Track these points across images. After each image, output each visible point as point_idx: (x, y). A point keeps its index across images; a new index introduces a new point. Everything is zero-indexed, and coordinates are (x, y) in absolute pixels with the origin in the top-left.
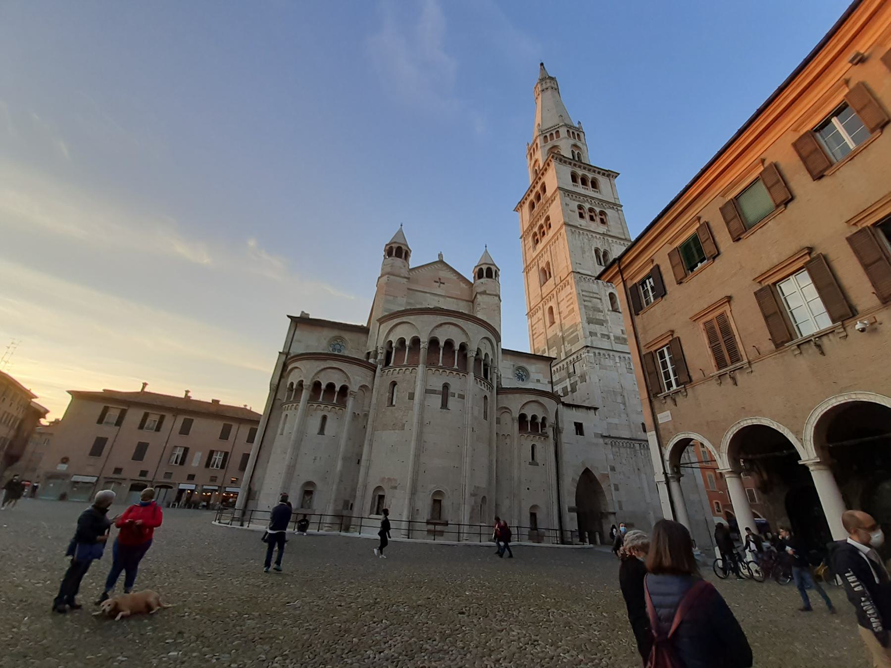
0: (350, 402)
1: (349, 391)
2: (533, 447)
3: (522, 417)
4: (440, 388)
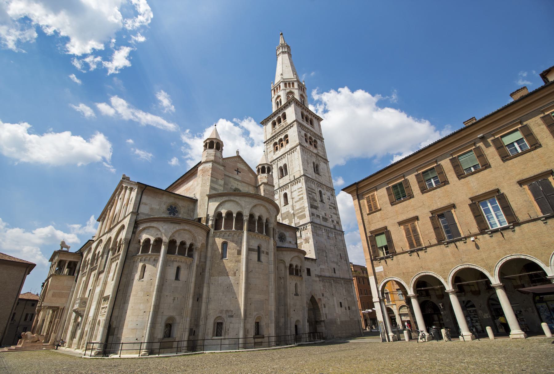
0: (196, 256)
1: (194, 247)
4: (256, 248)
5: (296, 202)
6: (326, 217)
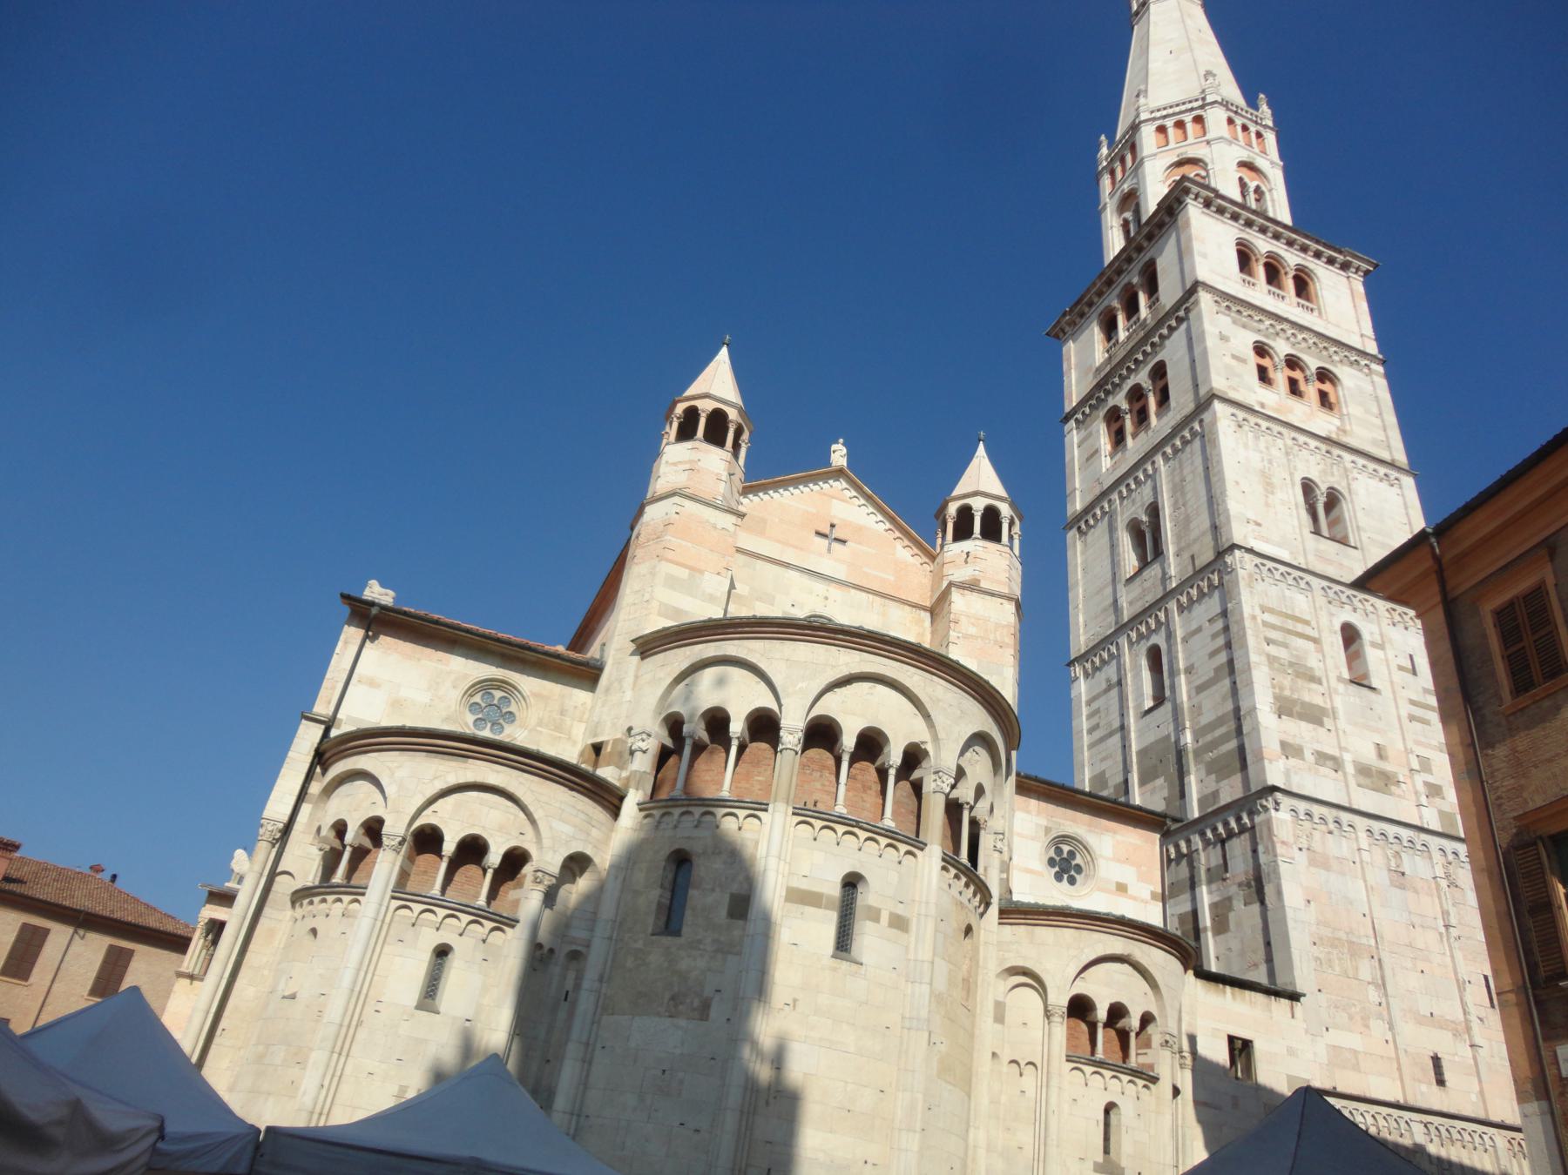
2: (1109, 1108)
3: (1080, 1008)
5: (1200, 689)
6: (1387, 767)
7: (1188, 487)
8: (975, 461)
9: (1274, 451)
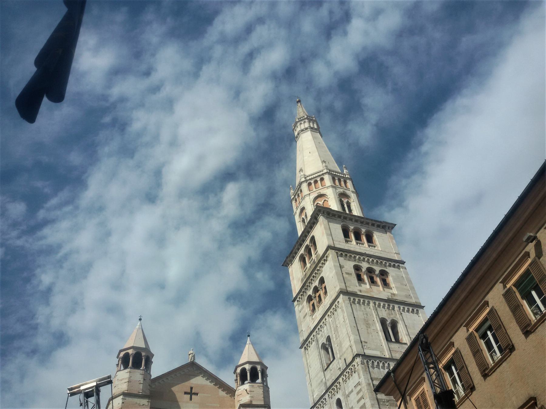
7: (339, 330)
8: (247, 346)
9: (368, 309)
